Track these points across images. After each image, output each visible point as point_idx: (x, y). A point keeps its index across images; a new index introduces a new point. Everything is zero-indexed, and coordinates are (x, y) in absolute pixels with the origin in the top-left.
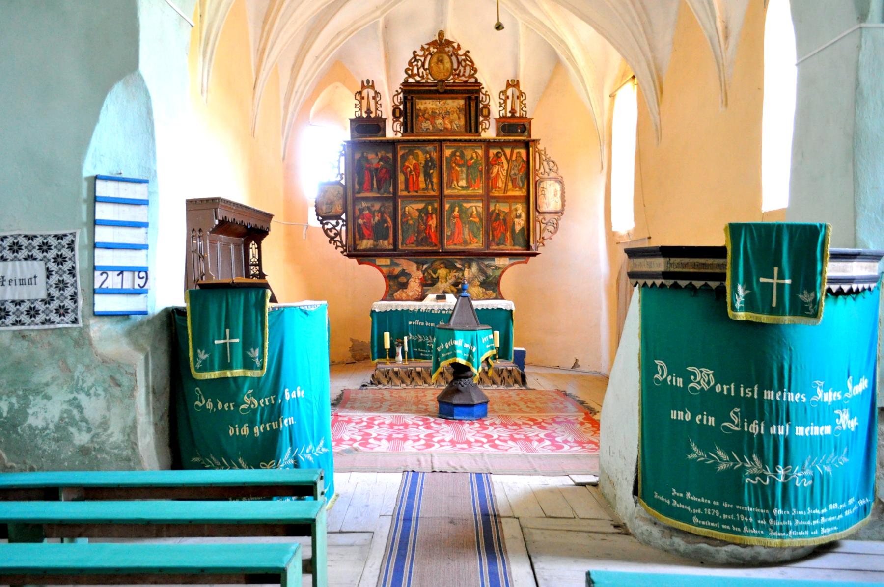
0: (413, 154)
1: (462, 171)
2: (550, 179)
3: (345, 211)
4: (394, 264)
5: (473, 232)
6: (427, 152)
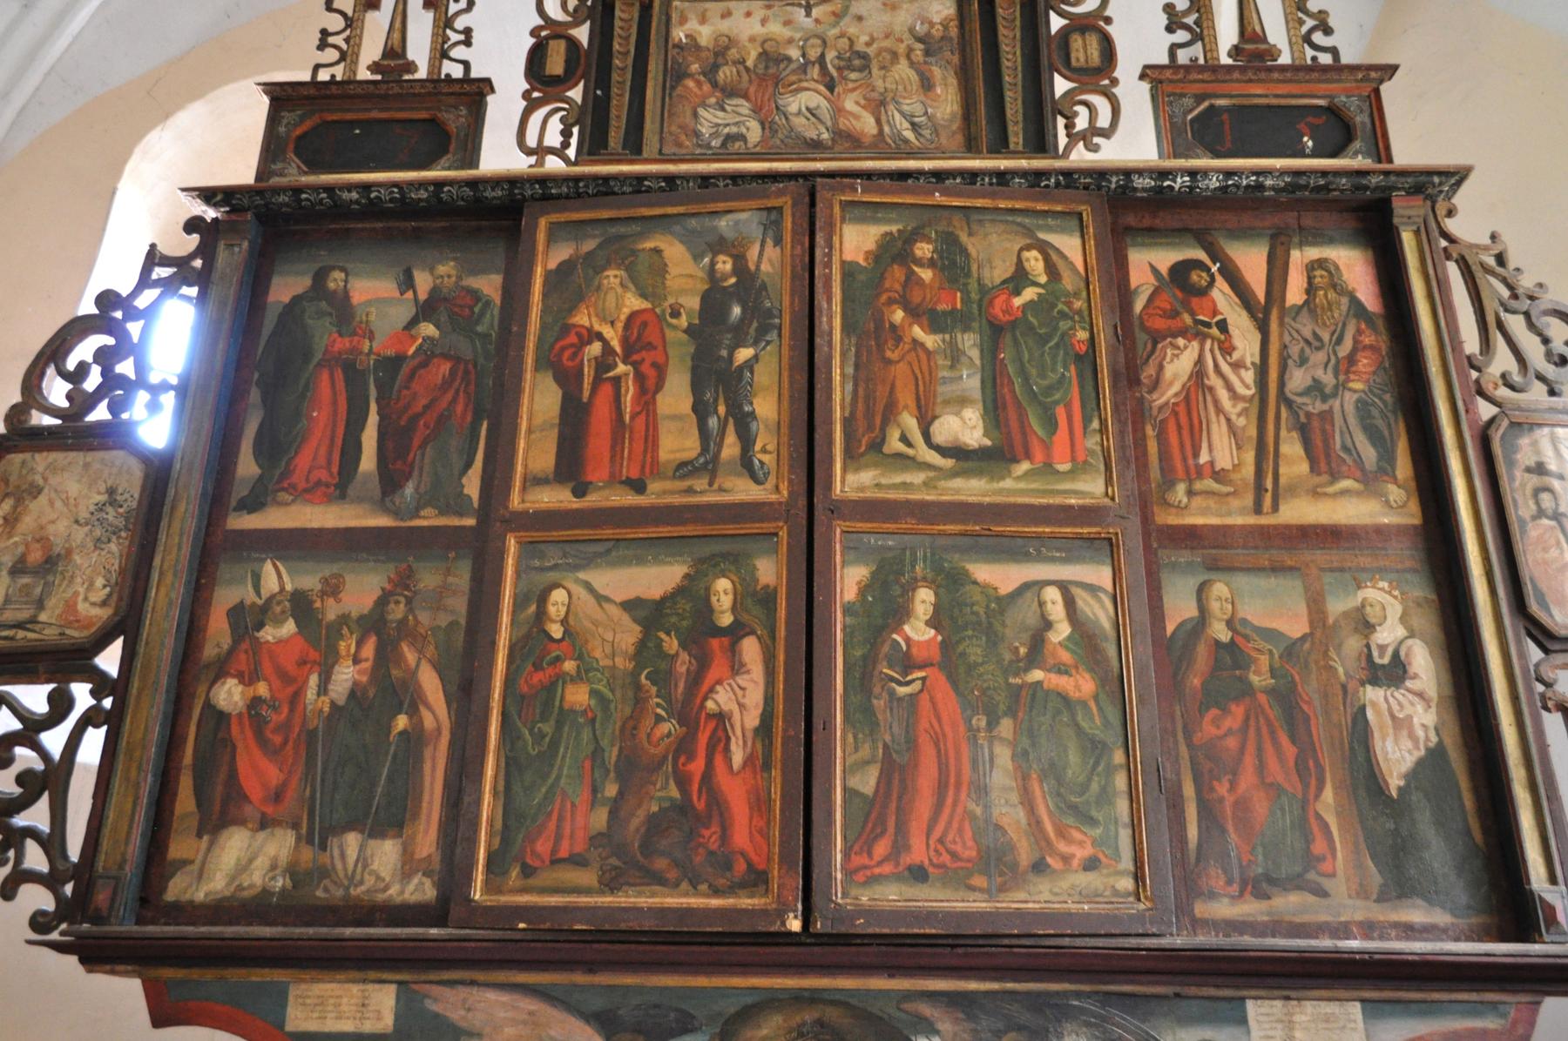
0: (627, 259)
1: (955, 356)
3: (126, 622)
5: (1053, 771)
6: (720, 245)
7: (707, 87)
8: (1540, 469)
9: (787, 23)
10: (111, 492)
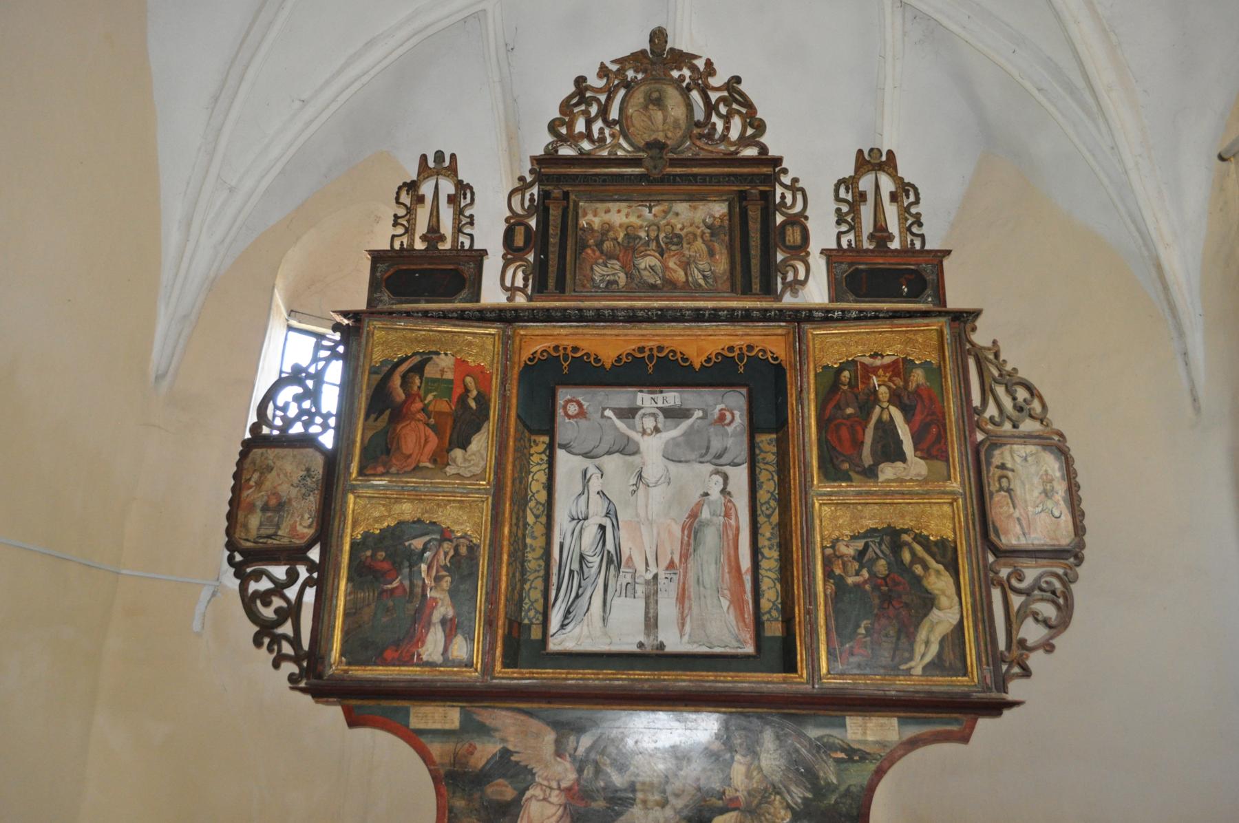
2: (1028, 438)
4: (472, 728)
7: (598, 253)
8: (1003, 467)
9: (639, 217)
10: (308, 470)
